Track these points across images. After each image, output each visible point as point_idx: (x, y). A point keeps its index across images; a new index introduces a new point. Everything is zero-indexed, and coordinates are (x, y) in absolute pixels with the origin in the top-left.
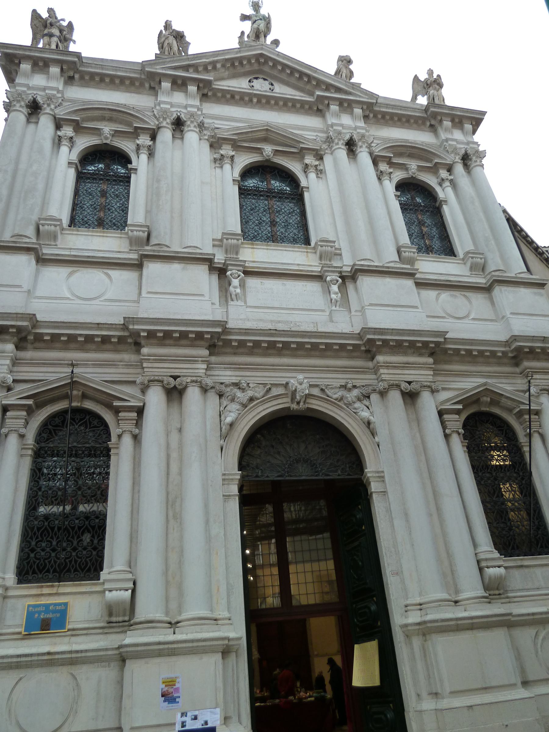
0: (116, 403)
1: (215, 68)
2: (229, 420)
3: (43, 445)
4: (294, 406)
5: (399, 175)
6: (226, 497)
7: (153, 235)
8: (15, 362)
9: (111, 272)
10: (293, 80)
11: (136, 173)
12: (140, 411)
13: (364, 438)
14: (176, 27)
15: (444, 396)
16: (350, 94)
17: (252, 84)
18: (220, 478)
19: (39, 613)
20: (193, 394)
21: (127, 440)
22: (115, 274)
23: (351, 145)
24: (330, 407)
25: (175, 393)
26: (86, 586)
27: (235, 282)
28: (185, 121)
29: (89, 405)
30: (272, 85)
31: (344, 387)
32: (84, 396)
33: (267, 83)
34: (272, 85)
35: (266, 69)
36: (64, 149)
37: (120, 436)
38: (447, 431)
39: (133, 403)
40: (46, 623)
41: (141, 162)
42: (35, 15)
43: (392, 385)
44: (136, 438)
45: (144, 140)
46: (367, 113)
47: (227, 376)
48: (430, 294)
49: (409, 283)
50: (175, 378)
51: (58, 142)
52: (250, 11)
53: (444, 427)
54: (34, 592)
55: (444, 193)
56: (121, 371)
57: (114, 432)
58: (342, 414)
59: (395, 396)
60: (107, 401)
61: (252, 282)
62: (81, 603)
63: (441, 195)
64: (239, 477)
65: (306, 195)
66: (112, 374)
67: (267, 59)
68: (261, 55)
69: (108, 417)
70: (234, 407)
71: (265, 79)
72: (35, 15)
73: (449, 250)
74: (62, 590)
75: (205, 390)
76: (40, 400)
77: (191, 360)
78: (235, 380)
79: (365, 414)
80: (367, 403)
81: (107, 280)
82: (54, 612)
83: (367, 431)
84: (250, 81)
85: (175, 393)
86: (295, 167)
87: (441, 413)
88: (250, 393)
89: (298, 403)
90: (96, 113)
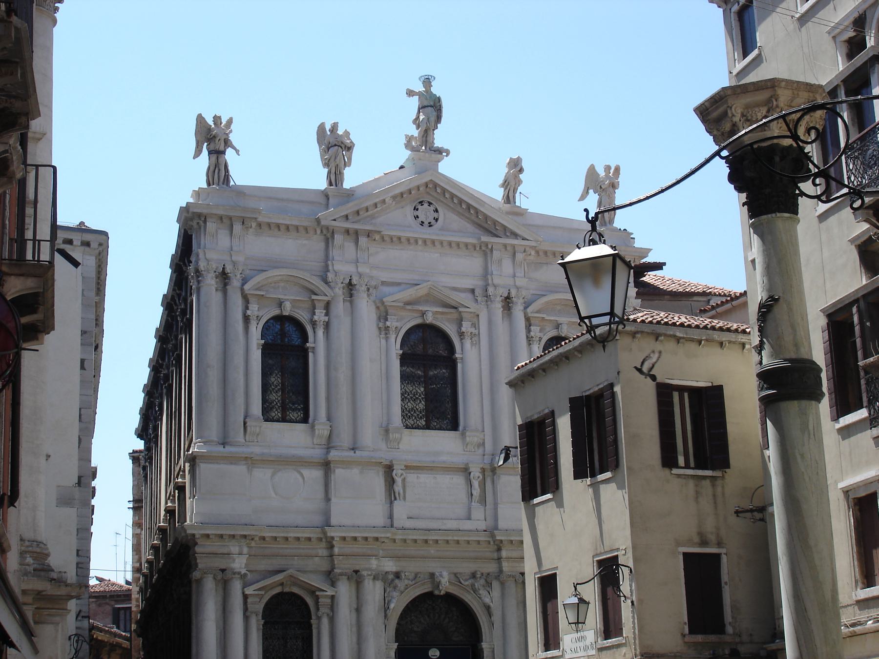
13: (484, 618)
16: (515, 235)
17: (416, 213)
21: (325, 621)
22: (306, 472)
23: (508, 301)
27: (399, 480)
29: (295, 590)
31: (473, 576)
33: (432, 208)
34: (436, 211)
42: (200, 119)
47: (390, 566)
52: (419, 88)
58: (470, 598)
60: (313, 591)
61: (412, 477)
65: (459, 366)
67: (436, 185)
70: (395, 594)
71: (430, 204)
72: (200, 119)
78: (394, 569)
79: (487, 600)
80: (489, 589)
81: (300, 479)
83: (486, 612)
86: (451, 330)
88: (406, 582)
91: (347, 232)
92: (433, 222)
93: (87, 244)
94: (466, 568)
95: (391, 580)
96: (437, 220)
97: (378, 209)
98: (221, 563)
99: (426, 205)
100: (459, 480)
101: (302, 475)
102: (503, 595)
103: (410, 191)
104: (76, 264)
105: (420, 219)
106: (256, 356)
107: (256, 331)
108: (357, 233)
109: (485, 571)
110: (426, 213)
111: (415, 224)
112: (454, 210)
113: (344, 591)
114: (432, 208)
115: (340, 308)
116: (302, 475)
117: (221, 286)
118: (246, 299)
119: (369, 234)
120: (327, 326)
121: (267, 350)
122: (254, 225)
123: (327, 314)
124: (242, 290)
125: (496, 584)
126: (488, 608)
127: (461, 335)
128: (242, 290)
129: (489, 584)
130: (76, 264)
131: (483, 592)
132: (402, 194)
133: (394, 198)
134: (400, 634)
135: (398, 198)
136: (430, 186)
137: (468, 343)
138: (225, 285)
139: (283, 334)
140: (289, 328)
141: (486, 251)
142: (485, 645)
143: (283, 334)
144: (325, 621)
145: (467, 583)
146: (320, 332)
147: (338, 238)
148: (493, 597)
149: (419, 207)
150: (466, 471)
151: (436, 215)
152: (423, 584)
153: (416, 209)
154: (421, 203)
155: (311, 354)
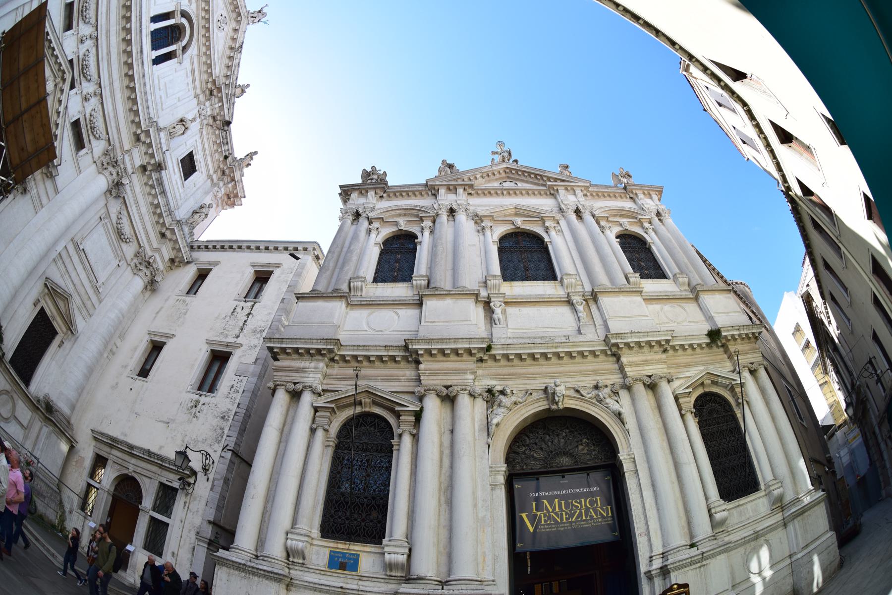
0: (398, 408)
2: (495, 421)
3: (342, 440)
4: (554, 407)
5: (617, 230)
6: (494, 486)
7: (432, 282)
8: (325, 376)
9: (399, 311)
12: (418, 416)
14: (449, 162)
15: (676, 383)
18: (488, 470)
19: (339, 557)
20: (464, 401)
21: (407, 440)
23: (577, 212)
24: (585, 405)
25: (449, 399)
26: (371, 548)
31: (597, 387)
32: (375, 403)
36: (373, 235)
37: (400, 435)
38: (683, 412)
39: (412, 408)
40: (342, 564)
43: (637, 380)
44: (416, 437)
46: (585, 192)
48: (656, 307)
49: (638, 299)
50: (447, 387)
53: (680, 410)
54: (332, 545)
55: (651, 238)
56: (403, 383)
57: (396, 431)
58: (596, 410)
59: (639, 389)
61: (511, 310)
62: (367, 558)
63: (648, 239)
64: (504, 469)
66: (396, 386)
69: (392, 420)
73: (663, 276)
74: (352, 547)
75: (472, 395)
76: (340, 405)
77: (462, 372)
79: (615, 407)
81: (396, 317)
82: (349, 559)
85: (449, 399)
87: (676, 398)
88: (514, 399)
89: (557, 403)
93: (305, 249)
94: (585, 383)
95: (491, 396)
98: (294, 376)
100: (565, 310)
101: (398, 314)
102: (633, 400)
104: (297, 258)
109: (609, 382)
113: (433, 407)
116: (398, 314)
125: (624, 394)
126: (619, 415)
127: (547, 230)
129: (616, 393)
130: (297, 258)
131: (611, 402)
134: (512, 454)
137: (553, 233)
141: (553, 194)
142: (622, 456)
144: (407, 440)
145: (590, 395)
147: (442, 191)
148: (624, 404)
150: (569, 302)
152: (537, 401)
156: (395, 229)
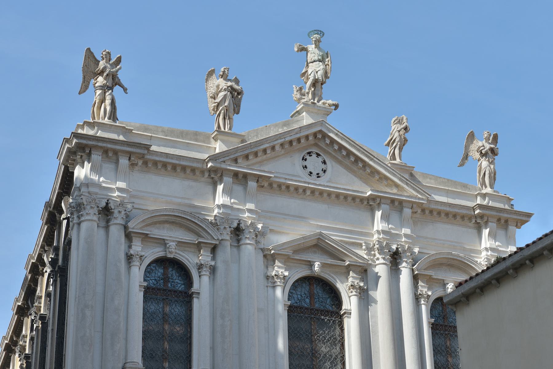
1: (273, 148)
10: (347, 162)
11: (198, 298)
17: (305, 163)
28: (244, 230)
30: (324, 162)
33: (320, 159)
34: (324, 162)
35: (322, 144)
41: (201, 284)
45: (205, 257)
51: (129, 258)
68: (320, 131)
71: (318, 155)
84: (303, 159)
90: (162, 218)
91: (236, 175)
92: (321, 173)
96: (325, 171)
97: (268, 156)
99: (314, 156)
103: (299, 140)
105: (309, 170)
106: (138, 297)
107: (137, 274)
108: (246, 176)
110: (314, 163)
111: (304, 175)
112: (340, 163)
114: (320, 159)
115: (226, 252)
117: (103, 224)
118: (128, 236)
119: (258, 178)
120: (213, 270)
121: (149, 293)
122: (140, 162)
123: (214, 258)
124: (126, 227)
128: (126, 227)
132: (291, 142)
133: (282, 145)
135: (287, 146)
136: (319, 136)
138: (108, 221)
139: (166, 279)
140: (173, 273)
143: (166, 279)
146: (206, 279)
149: (308, 157)
151: (323, 166)
153: (304, 159)
154: (309, 153)
155: (195, 300)
156: (161, 254)
